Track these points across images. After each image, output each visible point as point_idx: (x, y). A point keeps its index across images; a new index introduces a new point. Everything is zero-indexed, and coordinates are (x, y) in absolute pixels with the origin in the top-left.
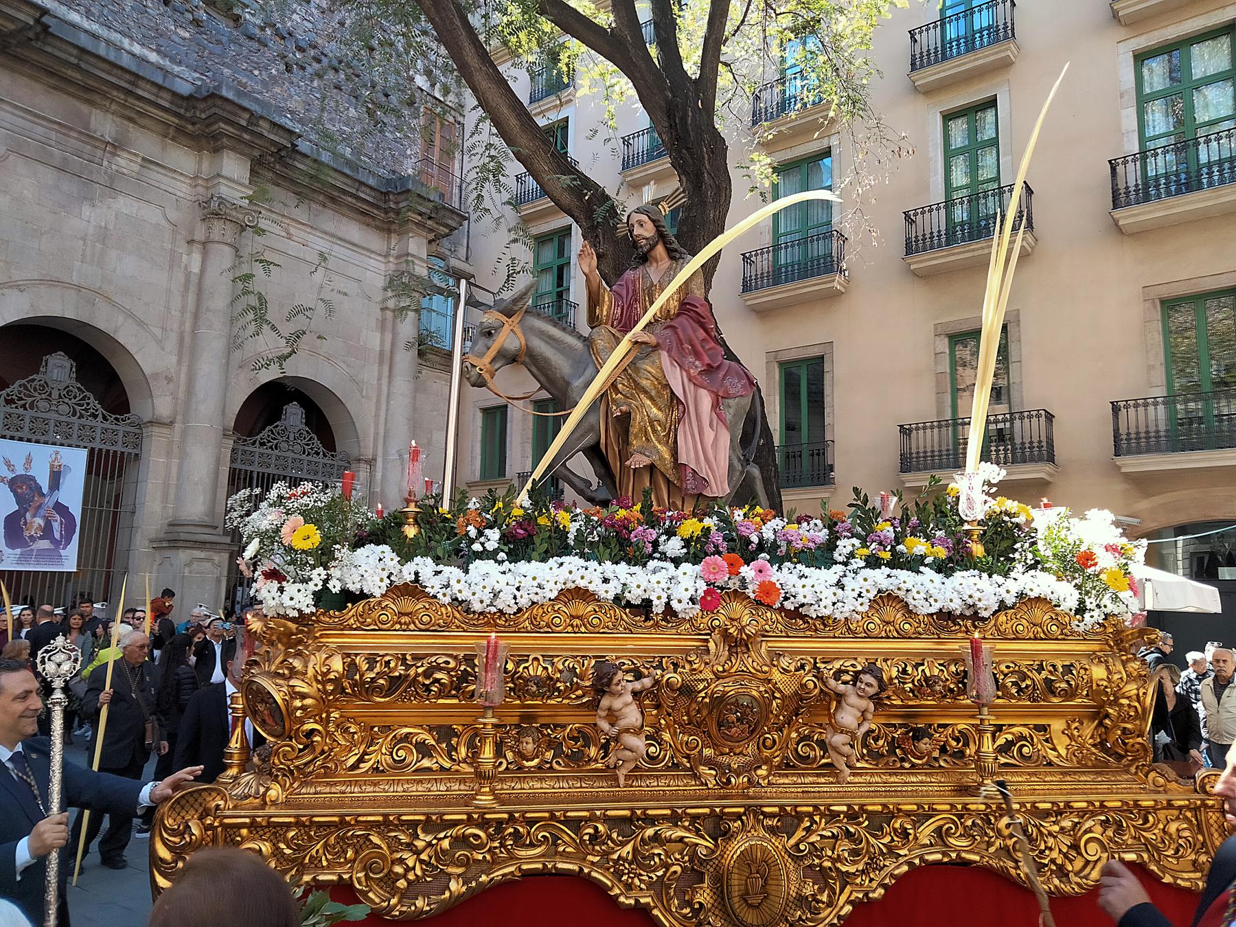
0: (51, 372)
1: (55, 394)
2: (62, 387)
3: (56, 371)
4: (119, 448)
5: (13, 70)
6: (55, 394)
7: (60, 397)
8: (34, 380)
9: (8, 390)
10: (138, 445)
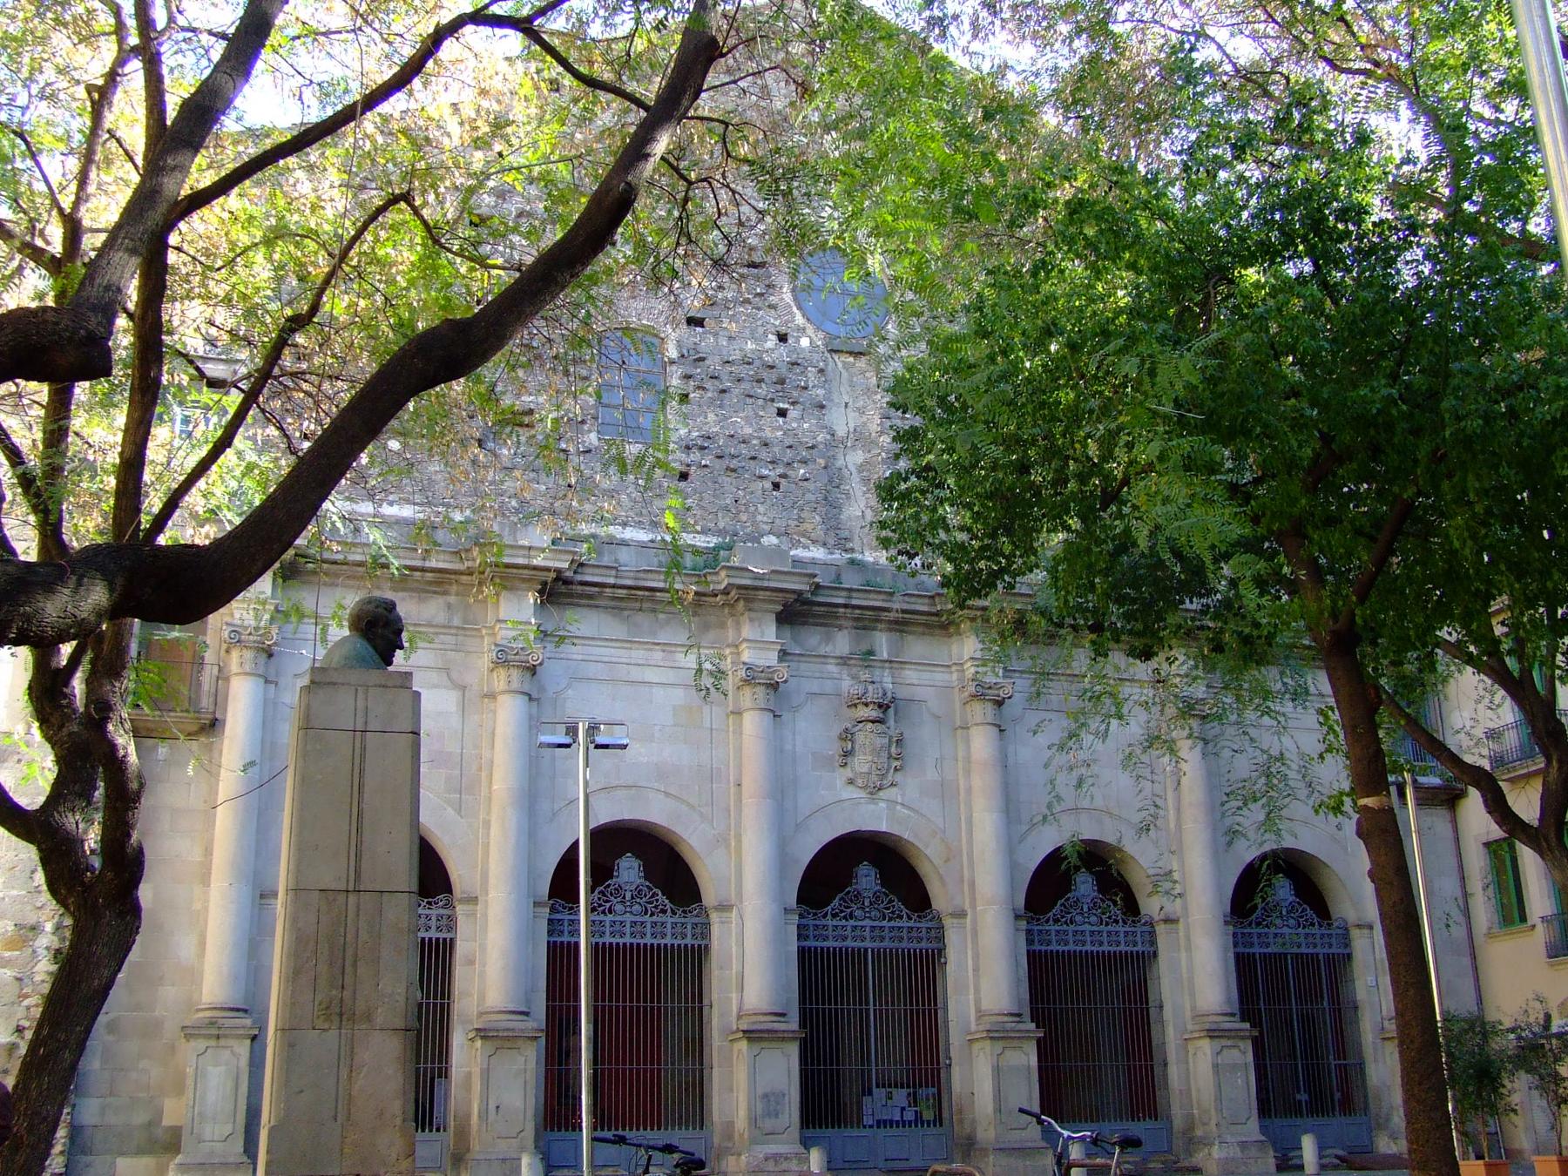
4: (1139, 948)
10: (1153, 943)
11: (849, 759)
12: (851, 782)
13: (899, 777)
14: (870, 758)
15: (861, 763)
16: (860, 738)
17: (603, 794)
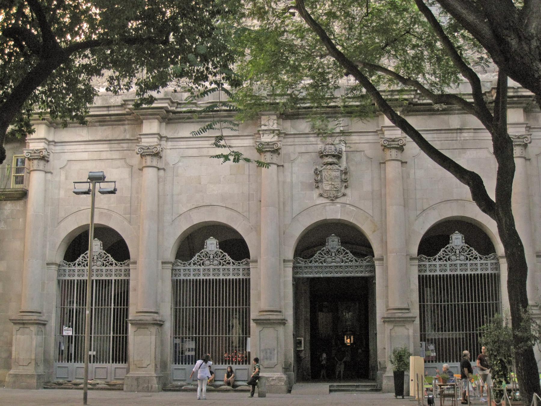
0: (454, 242)
1: (458, 252)
2: (459, 248)
3: (456, 241)
5: (416, 115)
6: (458, 252)
7: (460, 253)
8: (448, 247)
9: (439, 254)
11: (320, 185)
12: (321, 195)
13: (348, 191)
14: (330, 183)
15: (326, 186)
16: (324, 173)
17: (195, 210)
